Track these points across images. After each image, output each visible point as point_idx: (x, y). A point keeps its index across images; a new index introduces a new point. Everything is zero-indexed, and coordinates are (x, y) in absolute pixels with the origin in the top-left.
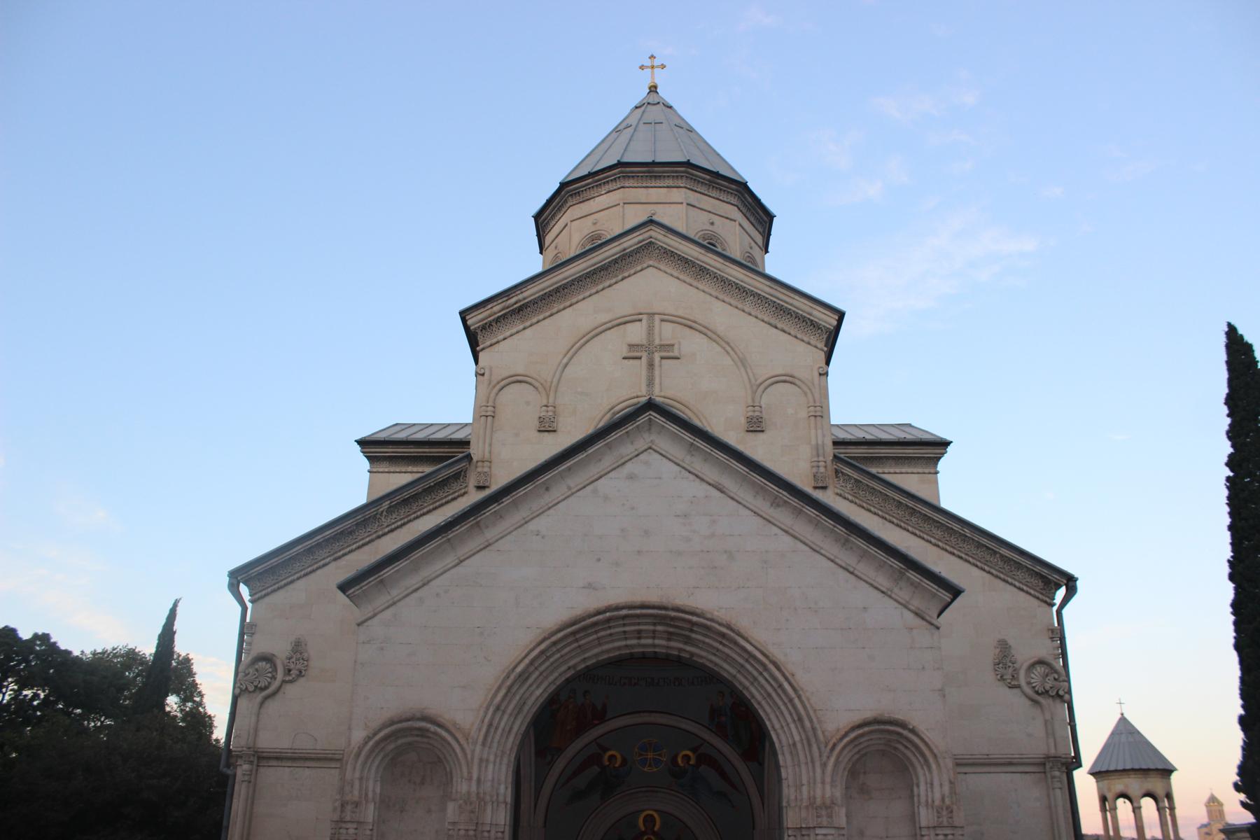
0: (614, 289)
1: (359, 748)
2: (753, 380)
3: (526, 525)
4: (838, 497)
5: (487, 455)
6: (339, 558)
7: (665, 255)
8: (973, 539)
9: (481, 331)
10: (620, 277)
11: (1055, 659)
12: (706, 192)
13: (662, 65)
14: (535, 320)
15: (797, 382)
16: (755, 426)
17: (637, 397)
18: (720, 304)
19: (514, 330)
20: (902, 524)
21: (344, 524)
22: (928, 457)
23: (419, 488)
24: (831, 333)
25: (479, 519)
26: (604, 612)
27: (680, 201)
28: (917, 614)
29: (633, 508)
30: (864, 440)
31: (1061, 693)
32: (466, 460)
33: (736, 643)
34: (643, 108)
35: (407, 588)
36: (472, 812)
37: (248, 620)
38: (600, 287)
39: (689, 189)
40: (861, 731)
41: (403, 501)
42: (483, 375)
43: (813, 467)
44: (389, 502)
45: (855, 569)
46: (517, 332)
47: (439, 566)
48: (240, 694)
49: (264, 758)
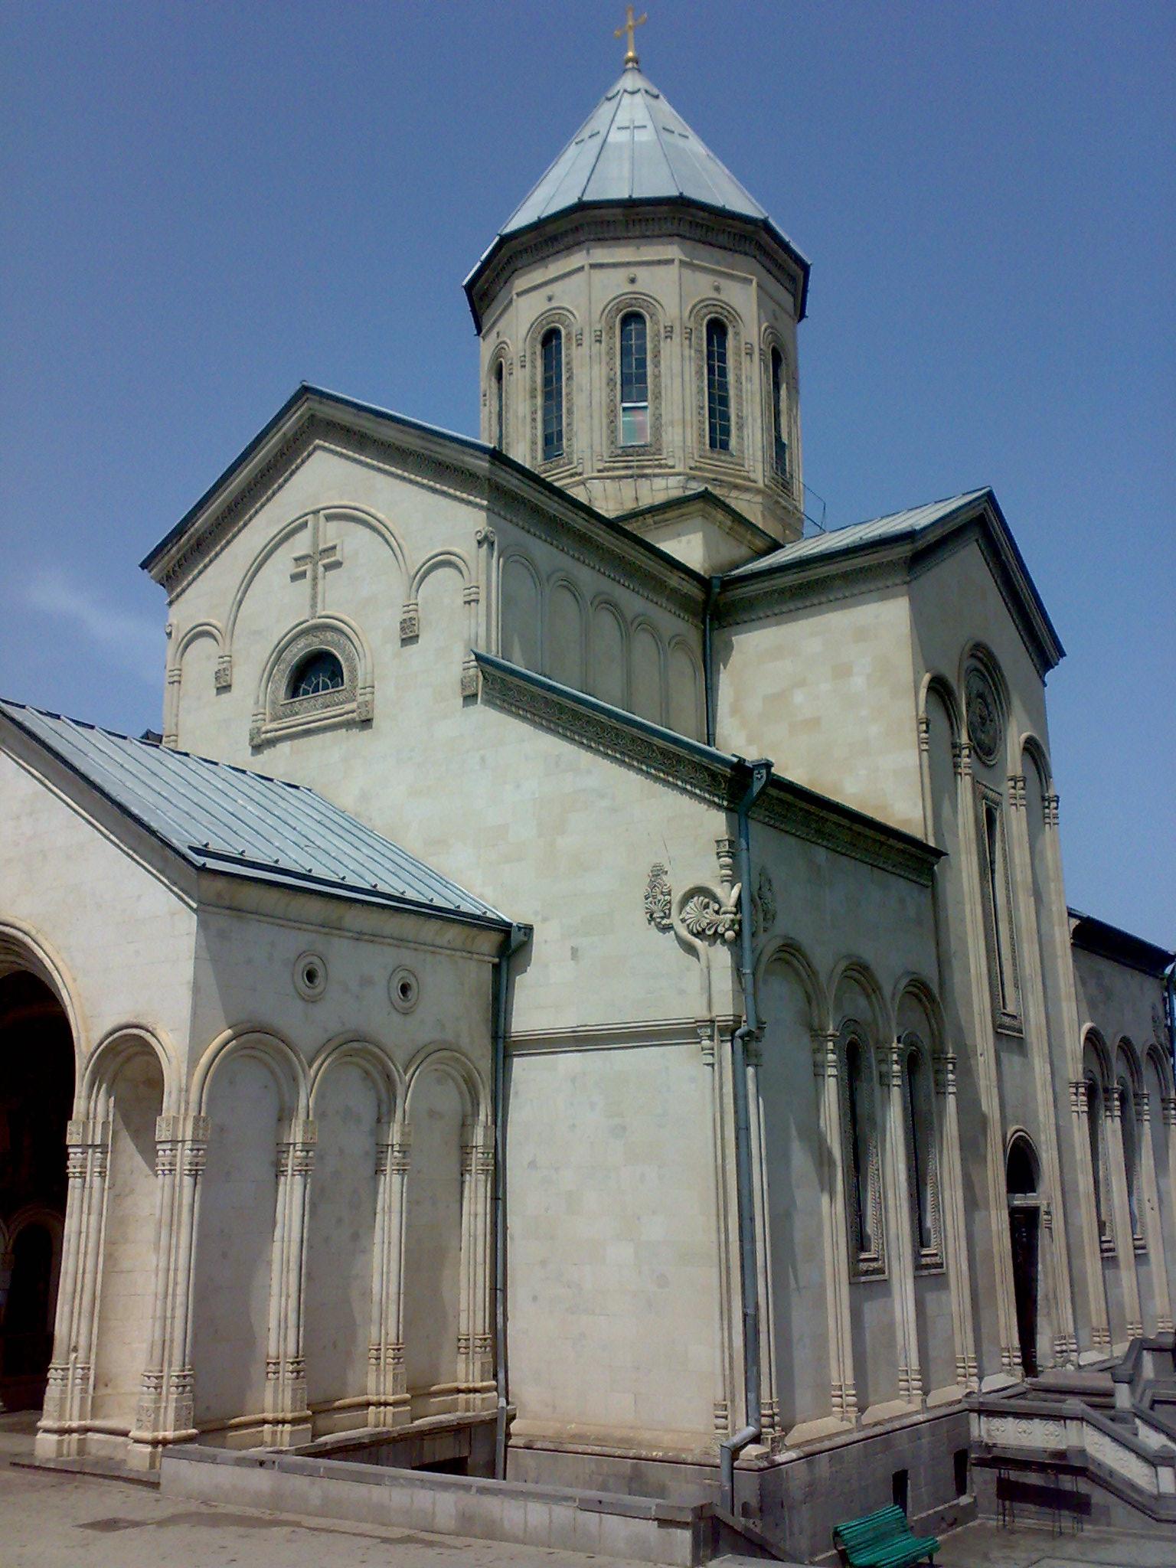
15: (453, 558)
18: (381, 477)
31: (721, 930)
34: (617, 99)
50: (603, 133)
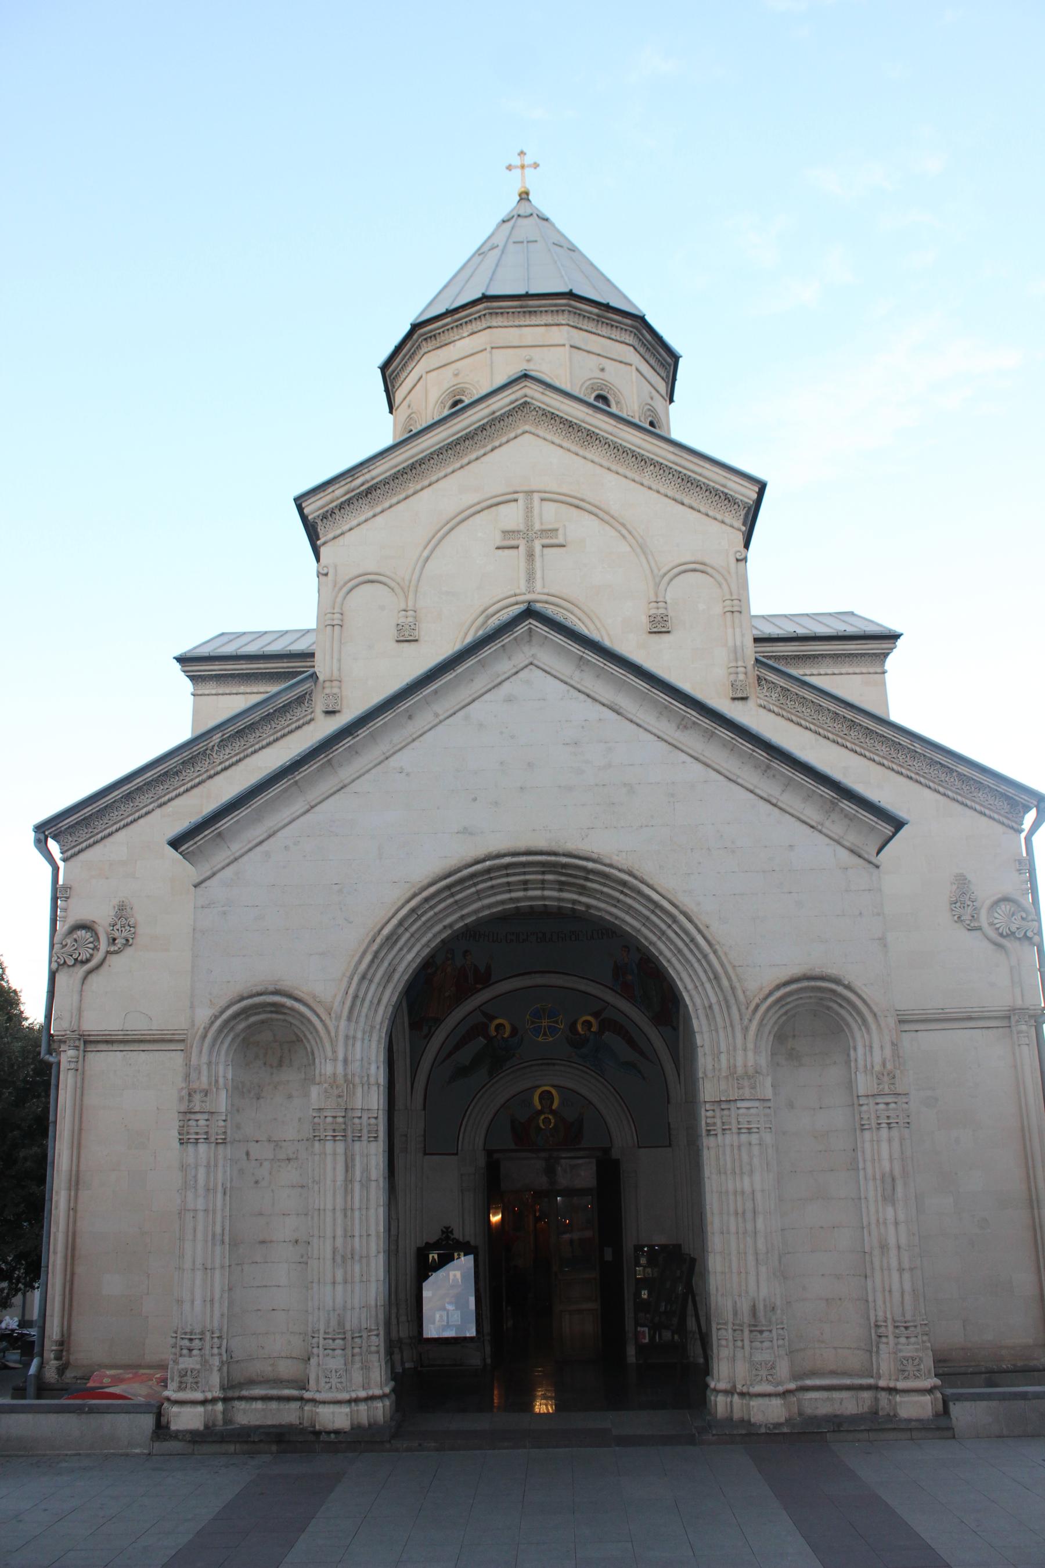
0: (482, 463)
1: (204, 1028)
2: (656, 571)
3: (386, 762)
4: (762, 710)
5: (336, 673)
6: (165, 803)
7: (544, 418)
8: (924, 756)
9: (322, 520)
10: (489, 448)
11: (1023, 894)
12: (594, 330)
13: (535, 163)
14: (387, 504)
15: (709, 570)
16: (659, 626)
17: (515, 596)
19: (362, 518)
20: (840, 740)
21: (168, 764)
22: (873, 653)
23: (256, 716)
24: (749, 508)
25: (331, 756)
26: (484, 860)
27: (562, 342)
28: (852, 851)
29: (513, 737)
30: (794, 635)
31: (1029, 934)
32: (311, 680)
33: (640, 892)
35: (250, 842)
36: (339, 1096)
37: (61, 882)
38: (465, 461)
39: (573, 327)
40: (788, 989)
41: (237, 732)
42: (326, 575)
43: (730, 674)
44: (220, 734)
45: (778, 799)
46: (366, 521)
47: (285, 814)
48: (57, 969)
49: (91, 1042)
50: (501, 245)
